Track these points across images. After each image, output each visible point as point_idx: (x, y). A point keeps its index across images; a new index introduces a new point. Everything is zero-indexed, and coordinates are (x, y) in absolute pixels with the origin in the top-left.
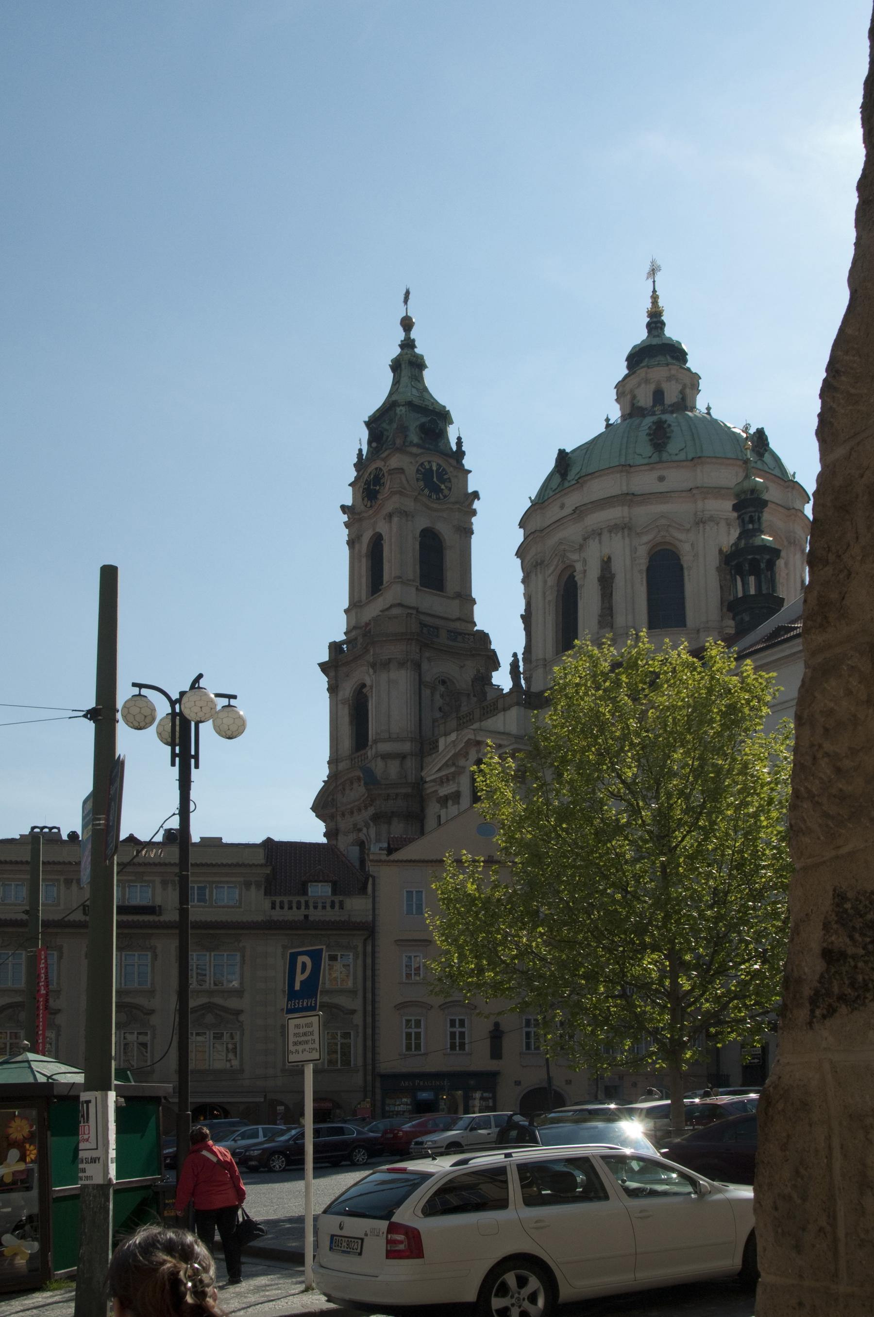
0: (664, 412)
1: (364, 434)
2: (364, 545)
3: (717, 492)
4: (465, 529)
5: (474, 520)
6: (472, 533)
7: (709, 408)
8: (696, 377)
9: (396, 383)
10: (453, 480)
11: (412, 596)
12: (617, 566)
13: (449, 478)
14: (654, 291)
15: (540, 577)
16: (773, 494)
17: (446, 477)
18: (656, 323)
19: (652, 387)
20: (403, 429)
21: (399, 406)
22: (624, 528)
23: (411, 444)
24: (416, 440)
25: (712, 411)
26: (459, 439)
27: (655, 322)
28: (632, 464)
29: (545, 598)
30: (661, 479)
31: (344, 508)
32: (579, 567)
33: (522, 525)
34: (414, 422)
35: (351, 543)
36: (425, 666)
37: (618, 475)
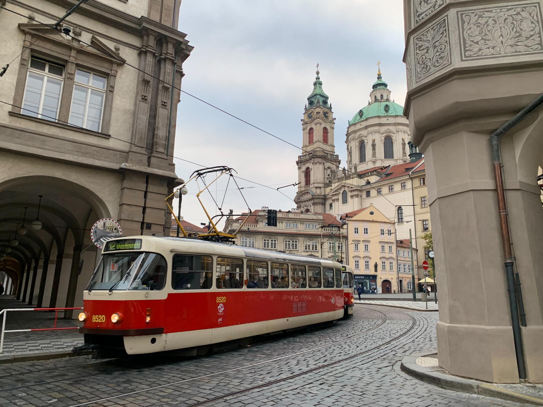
12: (377, 142)
20: (318, 102)
27: (379, 78)
30: (388, 120)
32: (366, 141)
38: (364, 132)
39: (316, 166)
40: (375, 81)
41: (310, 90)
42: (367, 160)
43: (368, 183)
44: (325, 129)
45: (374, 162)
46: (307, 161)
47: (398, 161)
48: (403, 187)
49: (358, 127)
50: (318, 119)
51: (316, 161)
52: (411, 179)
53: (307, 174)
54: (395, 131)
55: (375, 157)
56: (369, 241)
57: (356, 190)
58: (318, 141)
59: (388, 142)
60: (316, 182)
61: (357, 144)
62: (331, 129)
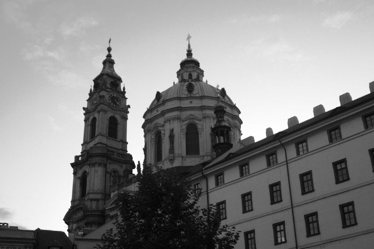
0: (192, 81)
1: (93, 84)
2: (90, 122)
3: (209, 108)
4: (125, 117)
5: (128, 115)
6: (127, 119)
7: (207, 81)
8: (202, 71)
9: (104, 68)
10: (121, 101)
11: (104, 140)
12: (176, 132)
13: (120, 100)
14: (189, 44)
15: (150, 135)
16: (228, 110)
17: (119, 99)
18: (189, 53)
19: (188, 73)
20: (105, 83)
21: (104, 75)
22: (178, 118)
23: (108, 88)
24: (109, 87)
25: (208, 82)
26: (124, 88)
28: (181, 97)
29: (151, 142)
30: (191, 102)
31: (84, 109)
32: (162, 132)
33: (144, 117)
34: (109, 81)
36: (108, 165)
37: (176, 100)
39: (93, 169)
42: (163, 158)
47: (205, 158)
49: (155, 113)
50: (101, 105)
51: (94, 162)
54: (200, 117)
55: (173, 153)
58: (101, 134)
59: (192, 133)
60: (91, 191)
61: (153, 137)
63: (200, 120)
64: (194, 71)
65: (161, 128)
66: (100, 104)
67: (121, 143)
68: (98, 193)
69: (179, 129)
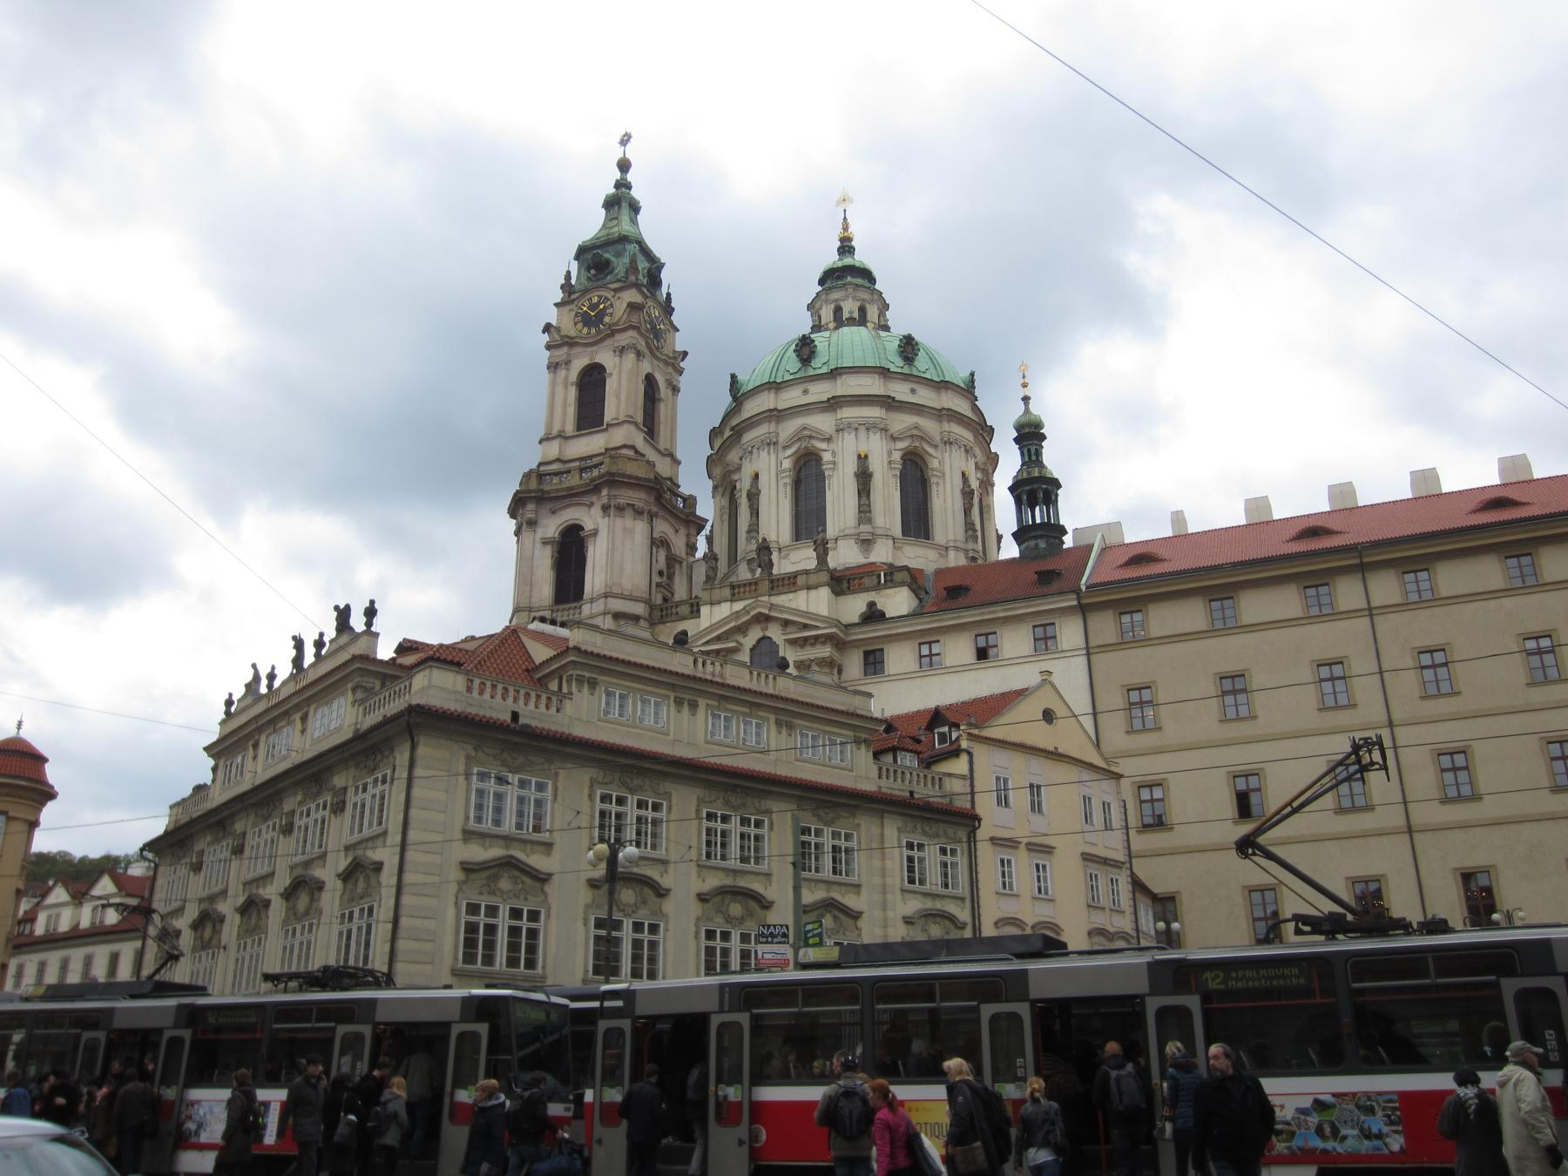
9: (608, 219)
12: (877, 466)
15: (773, 456)
26: (669, 295)
27: (846, 247)
30: (913, 391)
31: (548, 328)
32: (826, 457)
35: (553, 367)
38: (823, 422)
39: (619, 522)
40: (831, 258)
41: (590, 223)
43: (874, 615)
44: (650, 381)
45: (866, 543)
46: (573, 496)
47: (952, 553)
48: (1045, 641)
49: (792, 397)
50: (632, 333)
52: (1084, 610)
53: (570, 553)
55: (870, 521)
56: (1047, 850)
57: (828, 638)
60: (616, 590)
61: (787, 464)
62: (670, 392)
63: (936, 447)
64: (872, 302)
65: (823, 445)
66: (632, 327)
67: (668, 459)
68: (636, 600)
69: (884, 460)
